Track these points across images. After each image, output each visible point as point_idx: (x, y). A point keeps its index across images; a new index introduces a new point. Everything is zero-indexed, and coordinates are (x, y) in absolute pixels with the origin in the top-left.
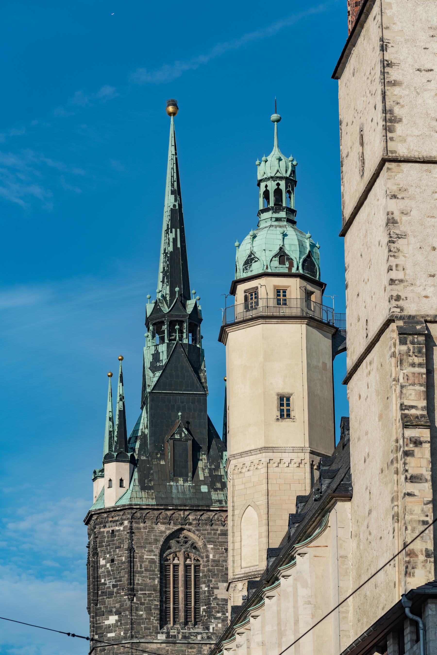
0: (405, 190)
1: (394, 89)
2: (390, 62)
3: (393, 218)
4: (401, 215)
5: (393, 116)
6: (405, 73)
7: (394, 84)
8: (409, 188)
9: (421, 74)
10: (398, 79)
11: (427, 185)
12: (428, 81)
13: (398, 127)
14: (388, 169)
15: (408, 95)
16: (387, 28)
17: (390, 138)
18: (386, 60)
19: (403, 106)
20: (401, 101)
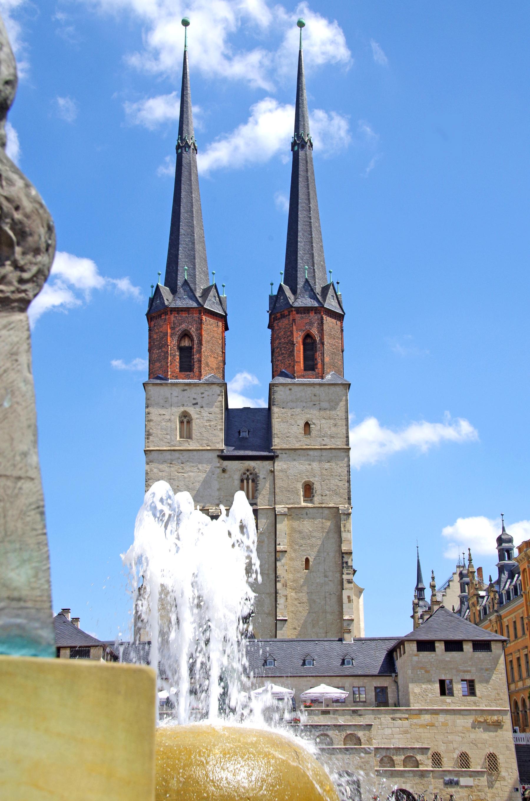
13: (151, 438)
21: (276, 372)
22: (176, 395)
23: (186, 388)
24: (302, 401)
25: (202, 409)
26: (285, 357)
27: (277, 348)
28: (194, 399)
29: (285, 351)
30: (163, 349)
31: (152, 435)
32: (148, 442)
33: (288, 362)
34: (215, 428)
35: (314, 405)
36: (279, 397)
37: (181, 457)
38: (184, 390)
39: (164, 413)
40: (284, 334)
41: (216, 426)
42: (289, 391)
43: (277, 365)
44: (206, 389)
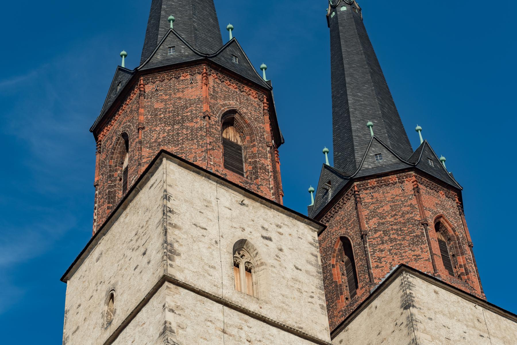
0: (182, 309)
1: (175, 230)
2: (171, 210)
3: (170, 327)
4: (178, 327)
5: (173, 249)
6: (184, 223)
7: (175, 226)
8: (185, 309)
9: (197, 228)
10: (178, 225)
11: (200, 312)
12: (203, 235)
14: (167, 287)
15: (186, 239)
16: (170, 186)
17: (170, 264)
18: (169, 208)
19: (181, 245)
20: (180, 241)
21: (379, 270)
22: (228, 204)
23: (247, 201)
24: (459, 320)
25: (281, 253)
26: (401, 244)
27: (376, 231)
28: (263, 228)
29: (398, 235)
30: (188, 124)
31: (179, 255)
32: (171, 266)
33: (413, 253)
34: (310, 300)
35: (481, 336)
36: (419, 295)
37: (246, 328)
38: (242, 204)
39: (204, 226)
40: (392, 210)
41: (312, 297)
42: (434, 294)
43: (380, 259)
44: (286, 223)
